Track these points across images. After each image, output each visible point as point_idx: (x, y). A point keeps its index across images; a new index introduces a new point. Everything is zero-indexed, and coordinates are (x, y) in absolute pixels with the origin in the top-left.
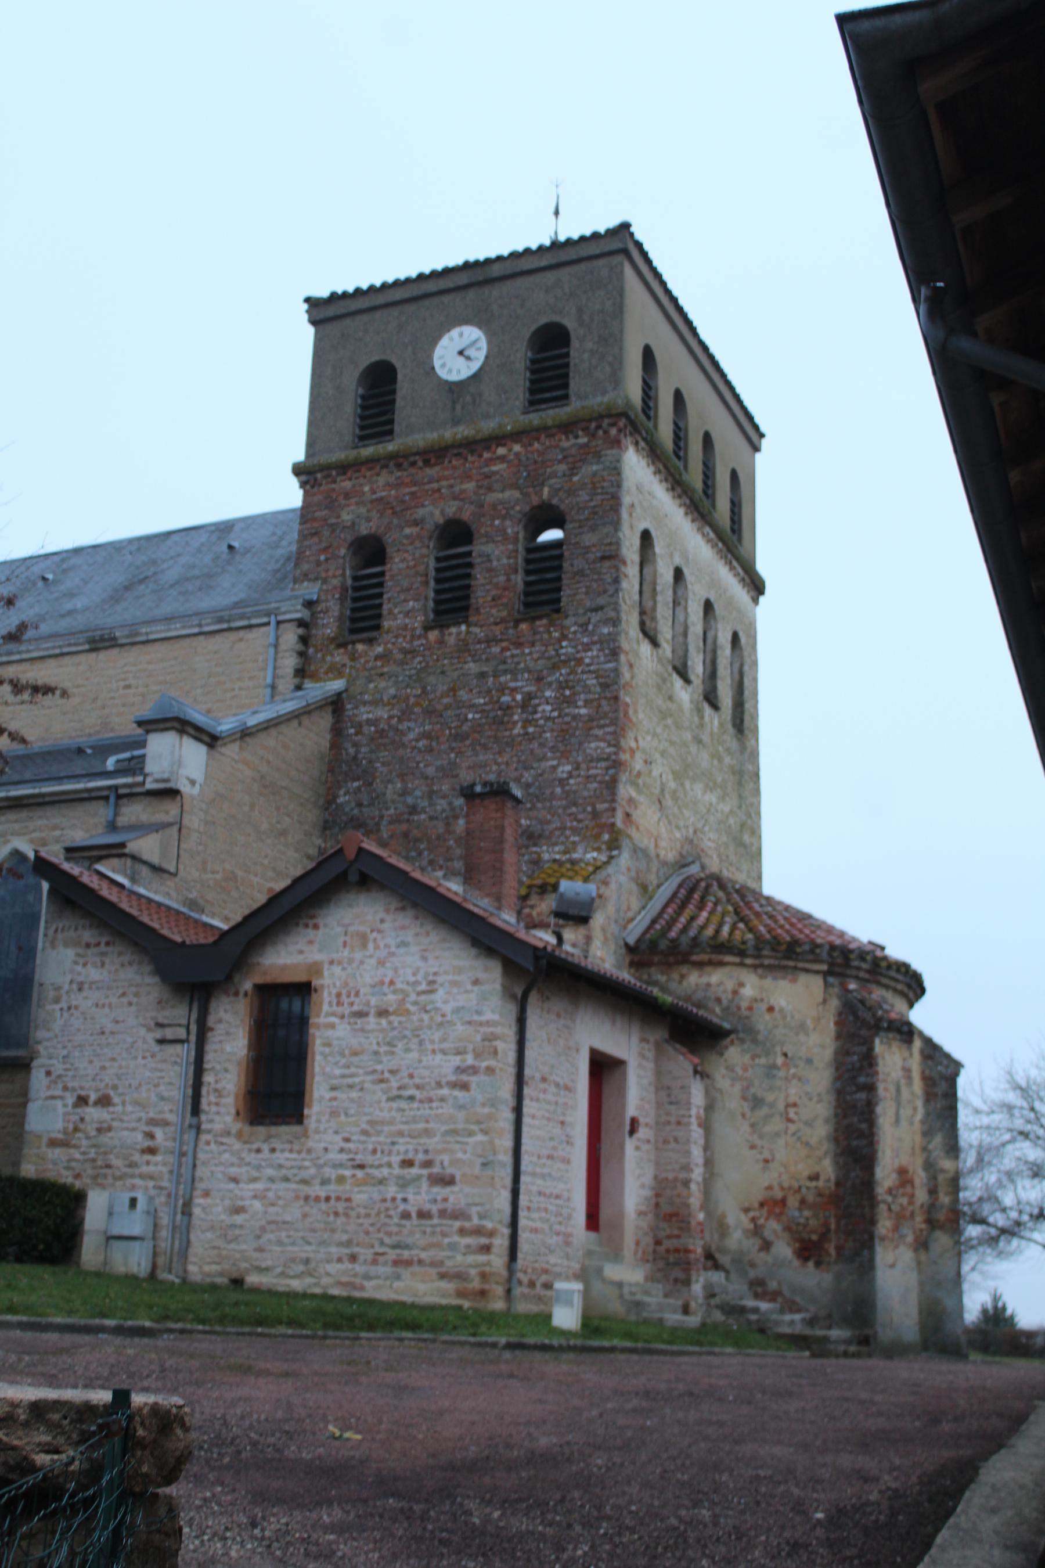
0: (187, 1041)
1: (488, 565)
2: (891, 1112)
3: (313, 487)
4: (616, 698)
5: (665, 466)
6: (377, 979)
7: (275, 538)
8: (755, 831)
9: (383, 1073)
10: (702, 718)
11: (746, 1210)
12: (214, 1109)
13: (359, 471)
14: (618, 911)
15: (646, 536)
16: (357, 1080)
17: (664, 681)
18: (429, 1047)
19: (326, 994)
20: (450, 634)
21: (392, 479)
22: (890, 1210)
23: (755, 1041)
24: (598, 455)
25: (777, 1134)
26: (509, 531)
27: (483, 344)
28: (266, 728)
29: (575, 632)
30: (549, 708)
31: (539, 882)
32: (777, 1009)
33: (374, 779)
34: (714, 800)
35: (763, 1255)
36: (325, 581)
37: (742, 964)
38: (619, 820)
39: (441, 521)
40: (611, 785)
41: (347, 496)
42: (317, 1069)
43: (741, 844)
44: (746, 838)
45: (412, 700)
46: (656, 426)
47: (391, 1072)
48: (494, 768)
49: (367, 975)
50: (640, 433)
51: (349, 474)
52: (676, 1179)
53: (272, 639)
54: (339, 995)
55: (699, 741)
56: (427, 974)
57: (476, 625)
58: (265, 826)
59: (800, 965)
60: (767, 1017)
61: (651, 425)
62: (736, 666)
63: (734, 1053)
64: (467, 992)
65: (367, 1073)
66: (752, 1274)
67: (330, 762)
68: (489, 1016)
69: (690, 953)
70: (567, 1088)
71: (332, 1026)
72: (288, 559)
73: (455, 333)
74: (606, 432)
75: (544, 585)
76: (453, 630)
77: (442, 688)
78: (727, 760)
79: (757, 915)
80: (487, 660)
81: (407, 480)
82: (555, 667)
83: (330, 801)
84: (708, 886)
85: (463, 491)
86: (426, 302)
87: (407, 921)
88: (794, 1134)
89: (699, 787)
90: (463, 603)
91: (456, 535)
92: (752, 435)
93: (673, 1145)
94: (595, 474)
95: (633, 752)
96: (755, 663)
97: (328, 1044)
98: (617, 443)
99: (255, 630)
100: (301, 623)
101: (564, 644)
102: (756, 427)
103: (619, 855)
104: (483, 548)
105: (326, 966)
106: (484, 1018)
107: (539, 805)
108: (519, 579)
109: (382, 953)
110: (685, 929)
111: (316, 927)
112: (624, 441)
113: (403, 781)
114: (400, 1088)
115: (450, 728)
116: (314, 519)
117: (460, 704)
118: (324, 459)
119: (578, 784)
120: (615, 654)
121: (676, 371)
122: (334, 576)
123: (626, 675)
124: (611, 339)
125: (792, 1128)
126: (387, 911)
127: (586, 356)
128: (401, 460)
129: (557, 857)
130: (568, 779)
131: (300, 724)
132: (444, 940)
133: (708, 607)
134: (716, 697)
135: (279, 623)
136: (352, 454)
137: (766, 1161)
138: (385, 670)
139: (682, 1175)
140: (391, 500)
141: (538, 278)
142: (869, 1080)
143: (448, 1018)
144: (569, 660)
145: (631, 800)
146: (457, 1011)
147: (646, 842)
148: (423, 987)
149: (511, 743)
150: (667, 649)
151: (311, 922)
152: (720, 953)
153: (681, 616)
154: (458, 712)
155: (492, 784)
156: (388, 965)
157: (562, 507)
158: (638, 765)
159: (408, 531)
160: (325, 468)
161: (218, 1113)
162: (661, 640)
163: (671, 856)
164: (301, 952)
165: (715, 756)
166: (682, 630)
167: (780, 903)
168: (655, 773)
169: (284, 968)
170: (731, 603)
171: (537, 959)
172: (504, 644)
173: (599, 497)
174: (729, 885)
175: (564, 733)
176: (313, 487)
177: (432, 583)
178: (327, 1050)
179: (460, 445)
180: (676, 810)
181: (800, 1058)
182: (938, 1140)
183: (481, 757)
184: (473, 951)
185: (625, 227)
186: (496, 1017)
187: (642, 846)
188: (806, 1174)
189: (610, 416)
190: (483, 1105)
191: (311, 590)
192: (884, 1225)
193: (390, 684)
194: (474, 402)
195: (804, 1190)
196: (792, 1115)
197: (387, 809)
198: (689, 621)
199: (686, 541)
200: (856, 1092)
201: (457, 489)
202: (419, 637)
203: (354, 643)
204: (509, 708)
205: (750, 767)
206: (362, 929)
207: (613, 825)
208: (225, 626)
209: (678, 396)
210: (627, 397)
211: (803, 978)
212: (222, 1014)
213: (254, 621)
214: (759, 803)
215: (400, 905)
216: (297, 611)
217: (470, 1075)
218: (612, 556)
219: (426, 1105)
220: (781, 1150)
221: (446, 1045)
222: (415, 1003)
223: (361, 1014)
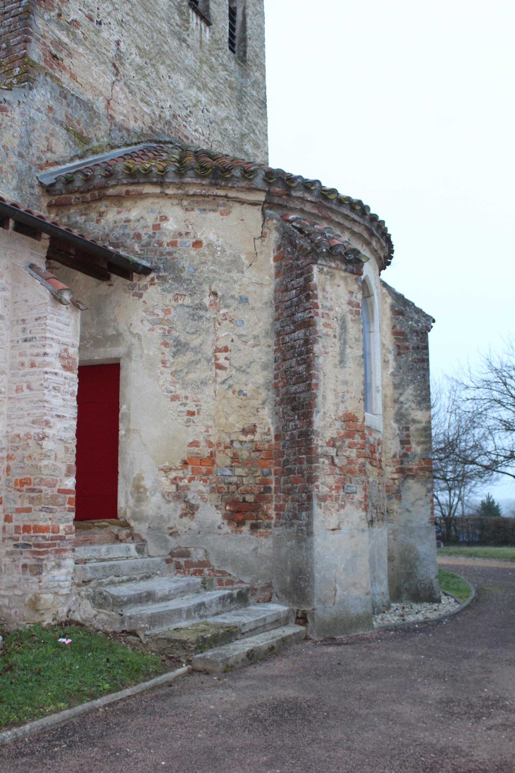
2: (334, 350)
11: (166, 471)
22: (333, 463)
23: (178, 279)
25: (204, 383)
32: (205, 243)
35: (185, 520)
52: (27, 435)
59: (232, 194)
60: (193, 253)
63: (154, 295)
66: (173, 543)
69: (105, 187)
88: (223, 382)
93: (26, 391)
125: (222, 375)
134: (209, 15)
137: (192, 414)
139: (36, 430)
142: (306, 315)
152: (138, 183)
181: (233, 297)
182: (410, 391)
188: (239, 426)
192: (325, 481)
195: (236, 445)
196: (222, 361)
200: (294, 332)
211: (237, 209)
220: (207, 399)
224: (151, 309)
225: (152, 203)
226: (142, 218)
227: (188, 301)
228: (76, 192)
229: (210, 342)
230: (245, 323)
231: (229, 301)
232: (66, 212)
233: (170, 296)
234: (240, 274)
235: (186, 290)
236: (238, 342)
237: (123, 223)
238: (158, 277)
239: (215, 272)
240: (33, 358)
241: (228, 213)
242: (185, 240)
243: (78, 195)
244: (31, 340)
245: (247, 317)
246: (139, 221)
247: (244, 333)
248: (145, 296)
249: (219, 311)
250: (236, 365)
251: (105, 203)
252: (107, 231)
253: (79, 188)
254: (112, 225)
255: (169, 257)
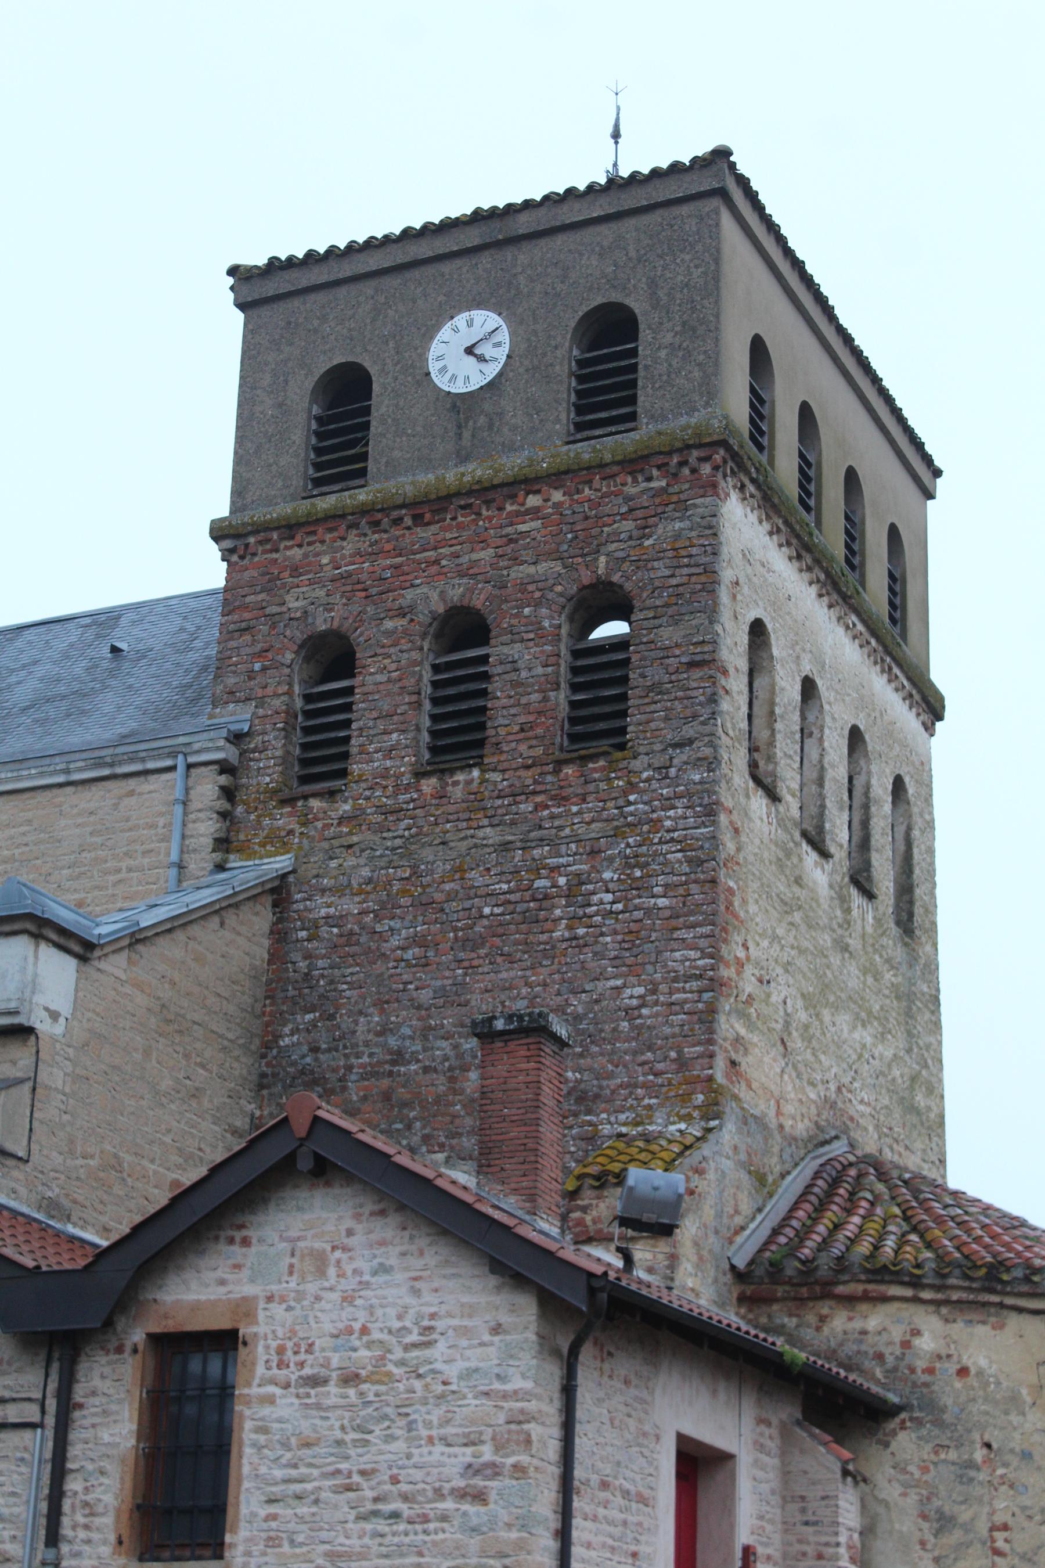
0: (41, 1425)
1: (513, 676)
3: (242, 558)
4: (714, 881)
5: (786, 523)
6: (341, 1326)
7: (184, 636)
8: (934, 1089)
9: (349, 1476)
10: (848, 911)
12: (82, 1534)
13: (314, 533)
14: (719, 1215)
15: (757, 629)
16: (309, 1486)
17: (788, 854)
18: (425, 1433)
19: (260, 1349)
20: (456, 783)
21: (364, 546)
23: (939, 1423)
24: (683, 506)
26: (546, 624)
27: (504, 336)
28: (169, 931)
29: (648, 780)
30: (609, 897)
31: (593, 1170)
32: (973, 1371)
33: (337, 1008)
34: (869, 1040)
36: (261, 702)
37: (916, 1300)
38: (719, 1072)
39: (441, 610)
40: (708, 1017)
41: (295, 570)
42: (246, 1469)
43: (913, 1109)
44: (920, 1100)
45: (396, 886)
46: (771, 461)
47: (363, 1473)
48: (524, 991)
49: (327, 1319)
50: (747, 473)
51: (298, 538)
53: (178, 793)
54: (281, 1350)
55: (845, 948)
56: (420, 1316)
57: (494, 770)
58: (166, 1084)
59: (1009, 1301)
60: (958, 1385)
61: (764, 458)
62: (901, 830)
63: (906, 1443)
64: (482, 1344)
65: (325, 1476)
67: (269, 982)
68: (518, 1383)
70: (643, 1500)
71: (271, 1400)
72: (205, 669)
73: (460, 320)
74: (694, 471)
75: (600, 707)
76: (460, 777)
77: (441, 868)
78: (888, 976)
79: (939, 1221)
80: (513, 823)
81: (388, 547)
82: (617, 834)
83: (269, 1043)
84: (860, 1176)
85: (474, 563)
86: (416, 273)
87: (389, 1234)
89: (844, 1019)
90: (478, 736)
91: (464, 630)
92: (922, 471)
94: (677, 536)
95: (740, 964)
96: (930, 826)
97: (263, 1430)
98: (712, 487)
99: (152, 778)
100: (225, 768)
101: (632, 798)
102: (928, 460)
103: (720, 1127)
104: (506, 650)
105: (262, 1304)
106: (509, 1387)
107: (595, 1049)
108: (561, 698)
109: (350, 1283)
110: (825, 1244)
111: (246, 1242)
112: (722, 484)
113: (382, 1011)
114: (376, 1500)
115: (455, 930)
116: (245, 607)
117: (471, 892)
118: (260, 514)
119: (656, 1015)
120: (710, 812)
121: (803, 374)
122: (276, 695)
123: (730, 846)
124: (701, 327)
126: (357, 1217)
127: (663, 354)
128: (379, 516)
129: (624, 1130)
130: (639, 1007)
131: (222, 924)
132: (447, 1262)
133: (855, 736)
134: (869, 879)
135: (190, 766)
136: (304, 507)
138: (355, 839)
140: (364, 577)
141: (588, 235)
143: (454, 1387)
144: (640, 823)
145: (738, 1040)
146: (468, 1374)
147: (762, 1107)
148: (414, 1337)
149: (550, 952)
150: (792, 805)
151: (238, 1235)
152: (882, 1282)
153: (813, 753)
154: (467, 904)
155: (520, 1018)
156: (359, 1302)
157: (628, 586)
158: (749, 985)
159: (389, 624)
160: (261, 528)
161: (88, 1542)
162: (783, 791)
163: (801, 1128)
164: (222, 1282)
165: (869, 970)
166: (815, 775)
167: (976, 1201)
168: (774, 999)
169: (196, 1307)
170: (891, 733)
171: (592, 1291)
172: (539, 799)
173: (686, 571)
174: (895, 1173)
175: (632, 938)
176: (242, 558)
177: (427, 705)
178: (262, 1439)
179: (470, 493)
180: (809, 1056)
181: (1012, 1451)
183: (504, 975)
184: (493, 1281)
185: (722, 154)
186: (529, 1385)
187: (756, 1112)
189: (700, 446)
190: (509, 1526)
191: (239, 716)
193: (362, 861)
194: (491, 427)
196: (1000, 1544)
197: (358, 1056)
198: (826, 761)
199: (820, 637)
201: (464, 559)
202: (407, 788)
203: (305, 798)
204: (546, 897)
205: (925, 988)
206: (318, 1245)
207: (710, 1079)
208: (106, 772)
209: (806, 413)
210: (726, 417)
211: (1014, 1321)
212: (97, 1382)
213: (151, 765)
214: (940, 1043)
215: (377, 1207)
216: (218, 749)
217: (487, 1478)
218: (705, 662)
219: (419, 1527)
221: (450, 1430)
222: (401, 1363)
223: (315, 1382)
224: (902, 1465)
225: (899, 1309)
226: (885, 1329)
227: (952, 1455)
228: (785, 1283)
229: (984, 1517)
230: (1030, 1490)
231: (1008, 1457)
232: (765, 1308)
233: (928, 1447)
234: (1020, 1418)
235: (951, 1438)
236: (1021, 1518)
237: (856, 1335)
238: (911, 1419)
239: (987, 1413)
240: (820, 1548)
241: (1000, 1326)
242: (947, 1365)
243: (787, 1288)
244: (815, 1523)
245: (1032, 1480)
246: (880, 1333)
247: (1028, 1503)
248: (894, 1446)
249: (994, 1471)
250: (1019, 1550)
251: (832, 1303)
252: (833, 1344)
253: (790, 1278)
254: (840, 1336)
255: (925, 1390)
